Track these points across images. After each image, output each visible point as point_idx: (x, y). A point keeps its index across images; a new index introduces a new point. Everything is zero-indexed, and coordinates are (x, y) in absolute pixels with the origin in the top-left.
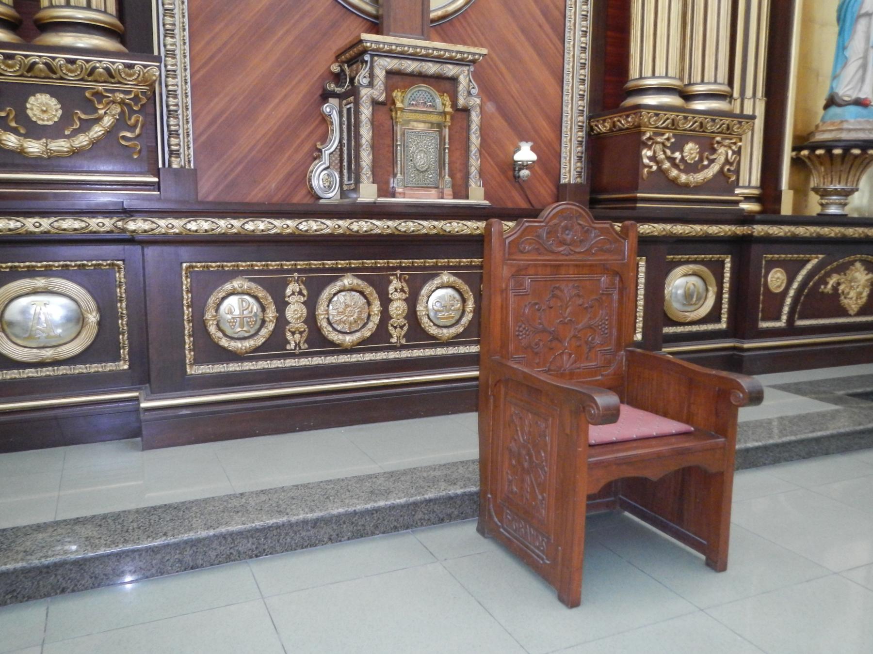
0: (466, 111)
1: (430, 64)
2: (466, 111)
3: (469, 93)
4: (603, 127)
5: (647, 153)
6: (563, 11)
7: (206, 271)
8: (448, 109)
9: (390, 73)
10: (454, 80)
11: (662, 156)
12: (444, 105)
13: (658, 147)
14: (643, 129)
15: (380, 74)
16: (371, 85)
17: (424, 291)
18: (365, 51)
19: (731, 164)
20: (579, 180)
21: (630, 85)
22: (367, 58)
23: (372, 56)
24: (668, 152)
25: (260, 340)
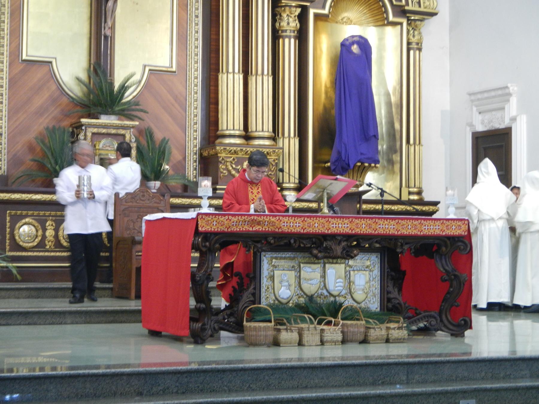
1: (112, 129)
4: (205, 154)
5: (222, 166)
7: (16, 215)
9: (93, 134)
11: (231, 168)
13: (228, 164)
14: (219, 155)
15: (89, 135)
16: (85, 139)
18: (82, 125)
19: (273, 171)
20: (195, 180)
21: (219, 133)
22: (83, 128)
23: (86, 128)
24: (234, 166)
25: (35, 244)
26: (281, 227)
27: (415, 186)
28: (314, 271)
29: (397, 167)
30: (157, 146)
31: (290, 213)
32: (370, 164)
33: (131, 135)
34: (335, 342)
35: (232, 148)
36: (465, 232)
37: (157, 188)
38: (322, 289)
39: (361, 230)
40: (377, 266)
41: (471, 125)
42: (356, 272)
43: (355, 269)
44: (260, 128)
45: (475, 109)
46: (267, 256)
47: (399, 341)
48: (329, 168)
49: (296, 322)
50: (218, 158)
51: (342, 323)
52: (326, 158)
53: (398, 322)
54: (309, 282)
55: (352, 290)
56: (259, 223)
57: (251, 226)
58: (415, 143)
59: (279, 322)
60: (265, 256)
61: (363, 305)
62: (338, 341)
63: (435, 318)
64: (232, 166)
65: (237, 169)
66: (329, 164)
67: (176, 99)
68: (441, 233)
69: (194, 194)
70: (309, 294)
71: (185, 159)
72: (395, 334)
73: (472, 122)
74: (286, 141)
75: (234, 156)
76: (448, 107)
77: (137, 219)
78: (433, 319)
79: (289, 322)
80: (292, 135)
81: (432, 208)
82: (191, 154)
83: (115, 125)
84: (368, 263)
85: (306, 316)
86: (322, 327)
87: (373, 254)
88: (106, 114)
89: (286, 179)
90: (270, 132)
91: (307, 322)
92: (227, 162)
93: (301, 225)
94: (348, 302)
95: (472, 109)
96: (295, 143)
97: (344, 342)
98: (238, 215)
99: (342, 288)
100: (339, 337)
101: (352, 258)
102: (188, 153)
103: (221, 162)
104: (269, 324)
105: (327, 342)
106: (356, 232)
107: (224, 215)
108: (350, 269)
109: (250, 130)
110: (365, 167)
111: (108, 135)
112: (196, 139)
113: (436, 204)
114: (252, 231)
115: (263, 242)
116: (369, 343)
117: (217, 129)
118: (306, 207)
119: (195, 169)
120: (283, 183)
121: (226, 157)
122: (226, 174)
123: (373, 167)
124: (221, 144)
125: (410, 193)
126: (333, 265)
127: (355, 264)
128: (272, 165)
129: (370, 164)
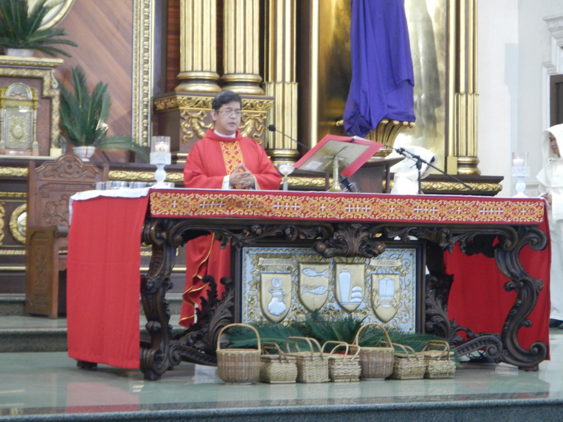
0: (50, 99)
1: (24, 70)
2: (50, 99)
3: (51, 88)
4: (161, 106)
5: (184, 125)
6: (131, 22)
8: (36, 98)
10: (41, 79)
11: (198, 127)
12: (33, 95)
13: (194, 121)
14: (181, 108)
17: (14, 213)
19: (259, 132)
20: (145, 144)
21: (180, 75)
24: (203, 124)
26: (271, 211)
27: (467, 154)
28: (319, 274)
29: (440, 127)
30: (90, 94)
31: (285, 190)
32: (401, 122)
33: (52, 79)
34: (349, 378)
35: (199, 98)
36: (540, 218)
37: (89, 156)
38: (331, 302)
39: (388, 215)
40: (411, 267)
41: (549, 65)
42: (381, 276)
43: (380, 272)
44: (240, 69)
45: (554, 41)
46: (251, 252)
47: (443, 376)
48: (341, 127)
49: (293, 349)
50: (179, 111)
51: (361, 350)
52: (337, 112)
53: (442, 349)
54: (313, 291)
55: (375, 303)
56: (239, 205)
57: (227, 209)
58: (467, 92)
59: (269, 349)
60: (248, 253)
61: (390, 325)
62: (354, 376)
63: (496, 343)
64: (200, 125)
65: (207, 128)
66: (341, 122)
67: (118, 25)
68: (505, 220)
69: (146, 166)
70: (312, 308)
71: (130, 113)
72: (438, 366)
73: (551, 62)
74: (279, 87)
75: (202, 110)
76: (515, 40)
77: (60, 201)
78: (492, 345)
79: (285, 350)
80: (288, 79)
81: (491, 186)
82: (139, 106)
83: (28, 63)
84: (398, 263)
85: (307, 339)
86: (331, 355)
87: (406, 250)
88: (16, 46)
89: (279, 144)
90: (255, 75)
91: (309, 350)
92: (193, 118)
93: (301, 207)
94: (369, 321)
95: (550, 43)
96: (292, 90)
97: (362, 377)
98: (209, 192)
99: (360, 300)
100: (357, 371)
101: (375, 255)
102: (136, 105)
103: (183, 119)
104: (254, 351)
105: (339, 377)
106: (380, 218)
107: (189, 192)
108: (373, 272)
109: (226, 72)
110: (394, 126)
111: (19, 78)
112: (146, 84)
113: (497, 180)
114: (229, 216)
115: (245, 231)
116: (400, 379)
117: (178, 71)
118: (307, 184)
119: (146, 128)
120: (274, 149)
121: (190, 111)
122: (192, 136)
123: (406, 126)
124: (184, 92)
125: (460, 165)
126: (347, 266)
127: (379, 265)
128: (259, 122)
129: (401, 122)
